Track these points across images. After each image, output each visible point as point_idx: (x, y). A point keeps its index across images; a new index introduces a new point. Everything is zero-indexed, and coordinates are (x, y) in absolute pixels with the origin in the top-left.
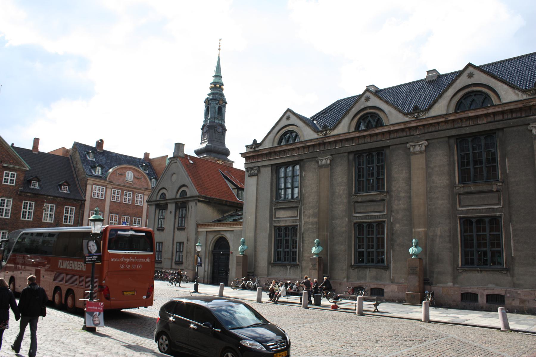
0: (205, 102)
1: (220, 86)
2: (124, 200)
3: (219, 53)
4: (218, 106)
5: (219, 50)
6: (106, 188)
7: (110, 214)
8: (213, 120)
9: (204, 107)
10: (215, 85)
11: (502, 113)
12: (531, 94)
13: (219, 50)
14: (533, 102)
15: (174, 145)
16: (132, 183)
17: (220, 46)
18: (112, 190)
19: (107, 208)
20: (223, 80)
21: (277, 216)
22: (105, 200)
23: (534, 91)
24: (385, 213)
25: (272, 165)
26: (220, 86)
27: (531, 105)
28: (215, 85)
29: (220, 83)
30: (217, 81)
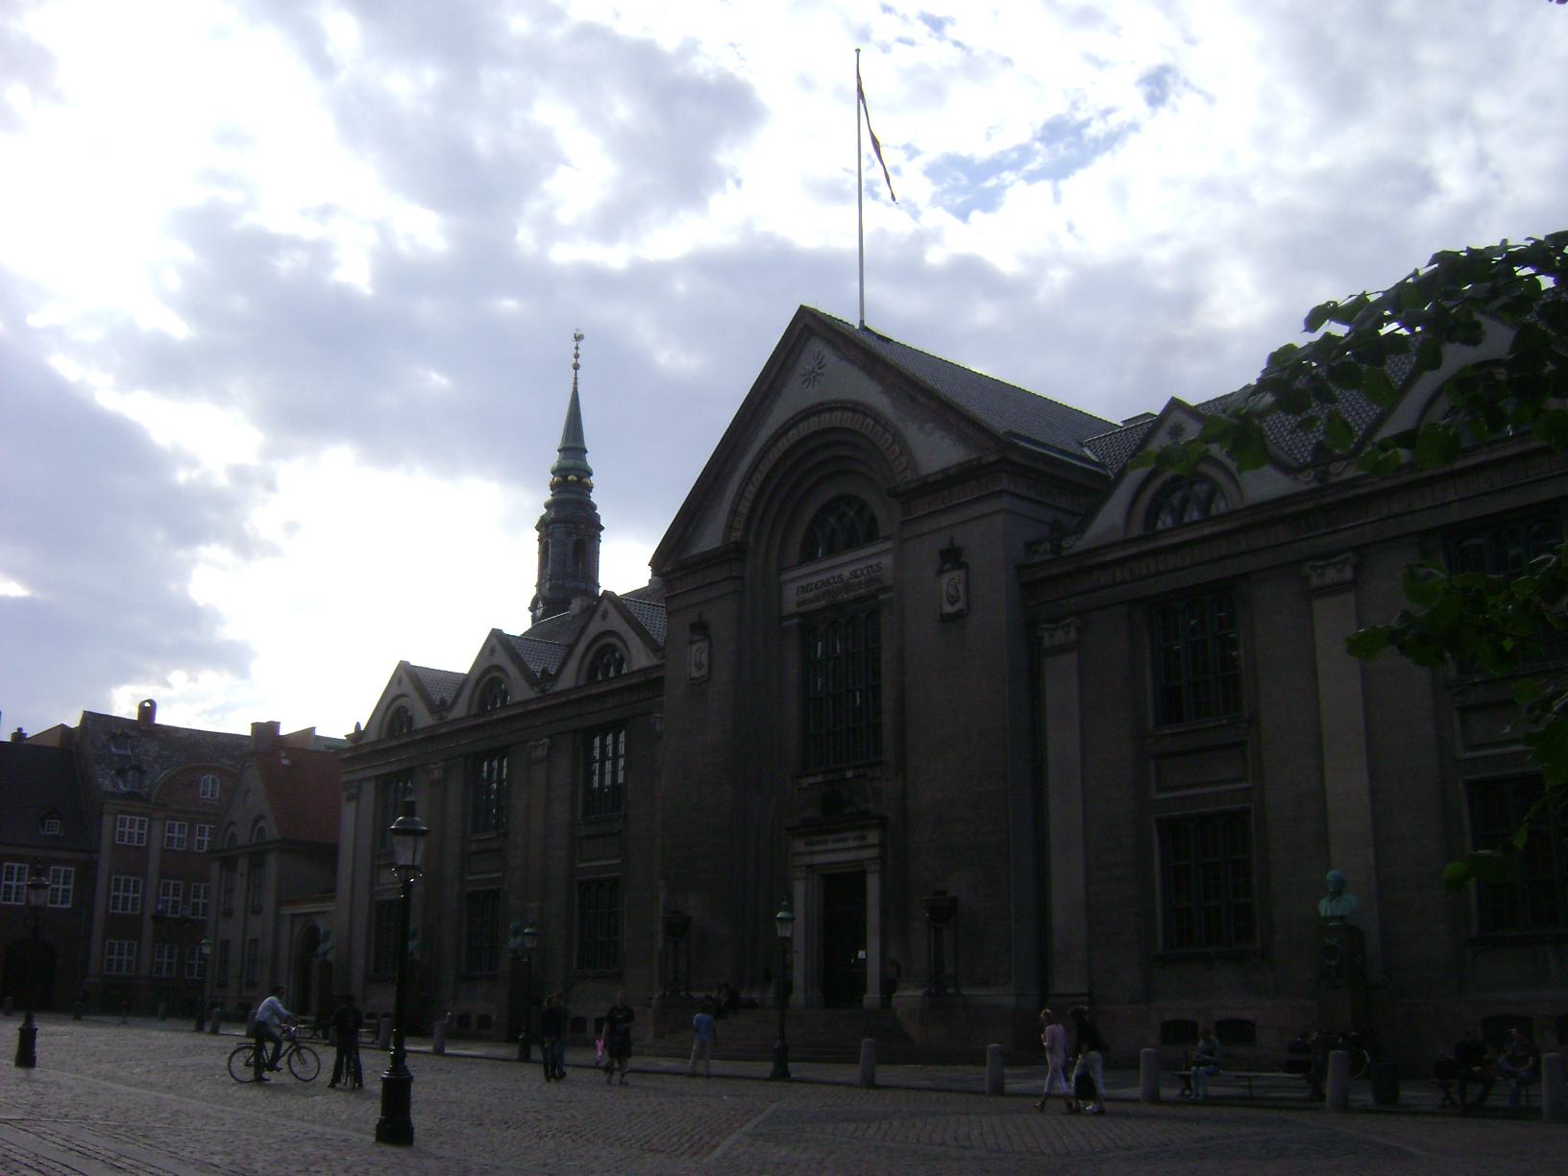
0: (538, 528)
1: (580, 479)
2: (196, 846)
3: (576, 378)
4: (575, 537)
5: (576, 367)
6: (151, 819)
7: (162, 881)
8: (560, 582)
9: (536, 545)
10: (565, 478)
11: (630, 688)
13: (576, 367)
15: (250, 726)
16: (215, 802)
17: (577, 356)
18: (165, 824)
19: (153, 866)
20: (591, 460)
21: (381, 882)
22: (147, 847)
24: (501, 874)
25: (377, 777)
26: (580, 479)
28: (565, 478)
29: (580, 470)
30: (570, 463)
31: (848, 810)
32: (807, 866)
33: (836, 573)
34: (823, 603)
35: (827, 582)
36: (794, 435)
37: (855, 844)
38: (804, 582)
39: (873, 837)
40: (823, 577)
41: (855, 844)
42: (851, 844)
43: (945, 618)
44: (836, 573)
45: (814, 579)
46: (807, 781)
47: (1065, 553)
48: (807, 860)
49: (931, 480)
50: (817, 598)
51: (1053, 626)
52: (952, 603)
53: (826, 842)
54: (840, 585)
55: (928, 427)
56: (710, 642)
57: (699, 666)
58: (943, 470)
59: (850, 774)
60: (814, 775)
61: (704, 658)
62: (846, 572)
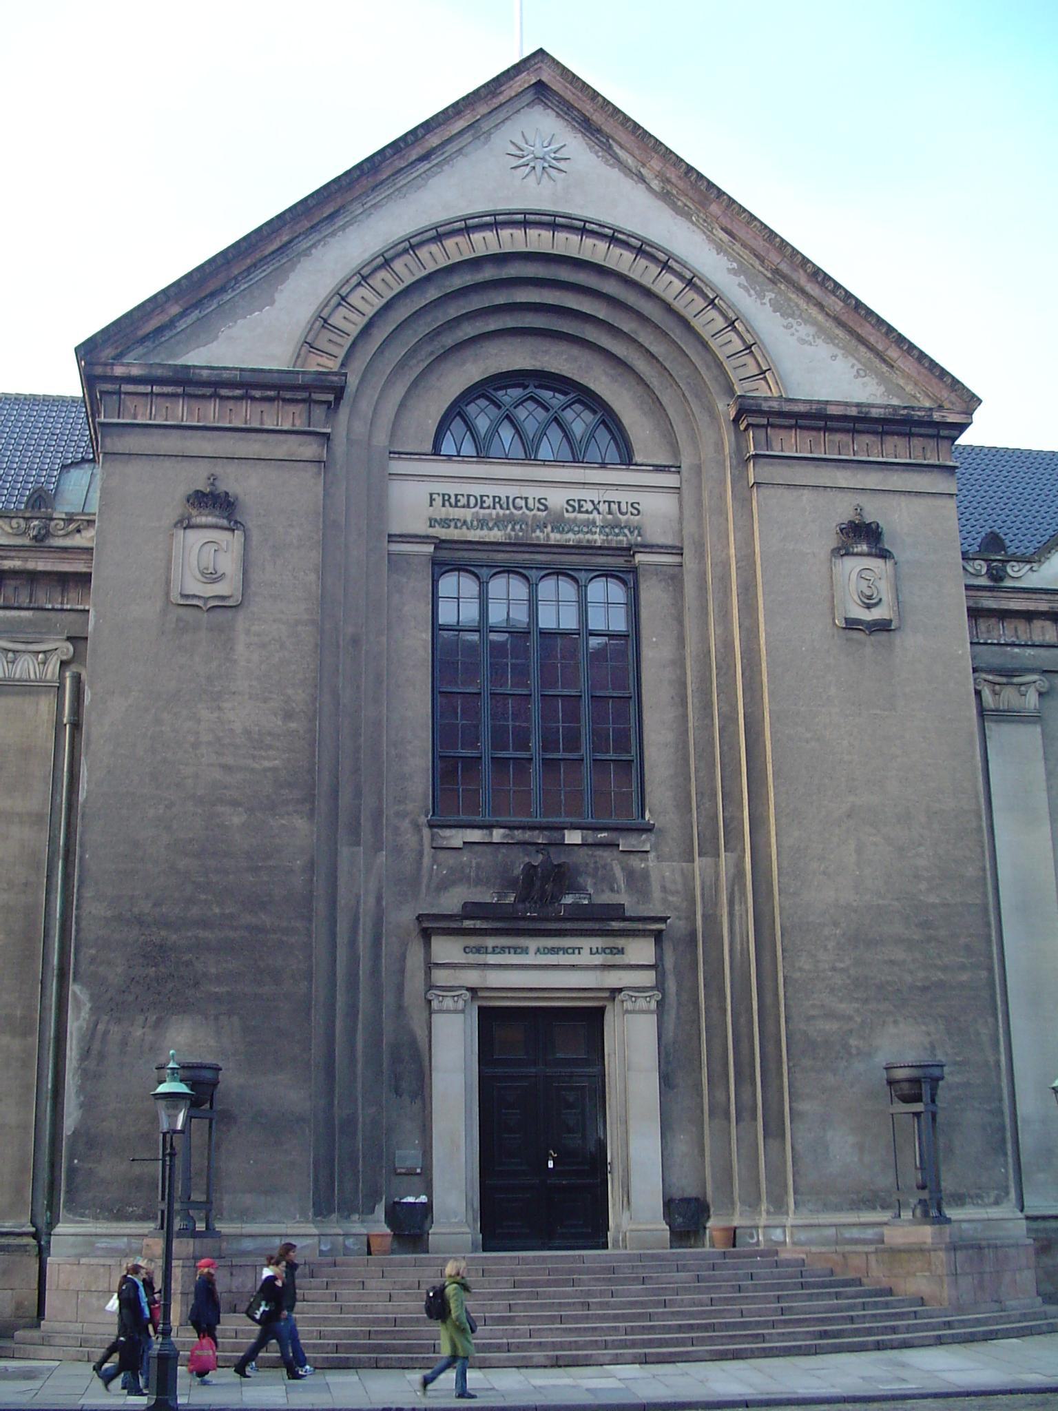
12: (10, 531)
14: (12, 558)
23: (21, 521)
27: (6, 568)
31: (568, 900)
32: (468, 989)
33: (533, 493)
34: (496, 535)
35: (511, 503)
36: (485, 243)
37: (598, 959)
38: (452, 489)
39: (641, 951)
40: (503, 491)
41: (598, 959)
42: (585, 958)
43: (852, 624)
44: (533, 493)
45: (477, 490)
46: (457, 837)
47: (1008, 583)
48: (472, 978)
49: (832, 410)
50: (482, 523)
51: (1004, 680)
52: (869, 607)
53: (525, 951)
54: (545, 513)
55: (805, 330)
56: (247, 538)
57: (213, 577)
58: (858, 405)
59: (573, 837)
60: (489, 827)
61: (229, 564)
62: (557, 499)
